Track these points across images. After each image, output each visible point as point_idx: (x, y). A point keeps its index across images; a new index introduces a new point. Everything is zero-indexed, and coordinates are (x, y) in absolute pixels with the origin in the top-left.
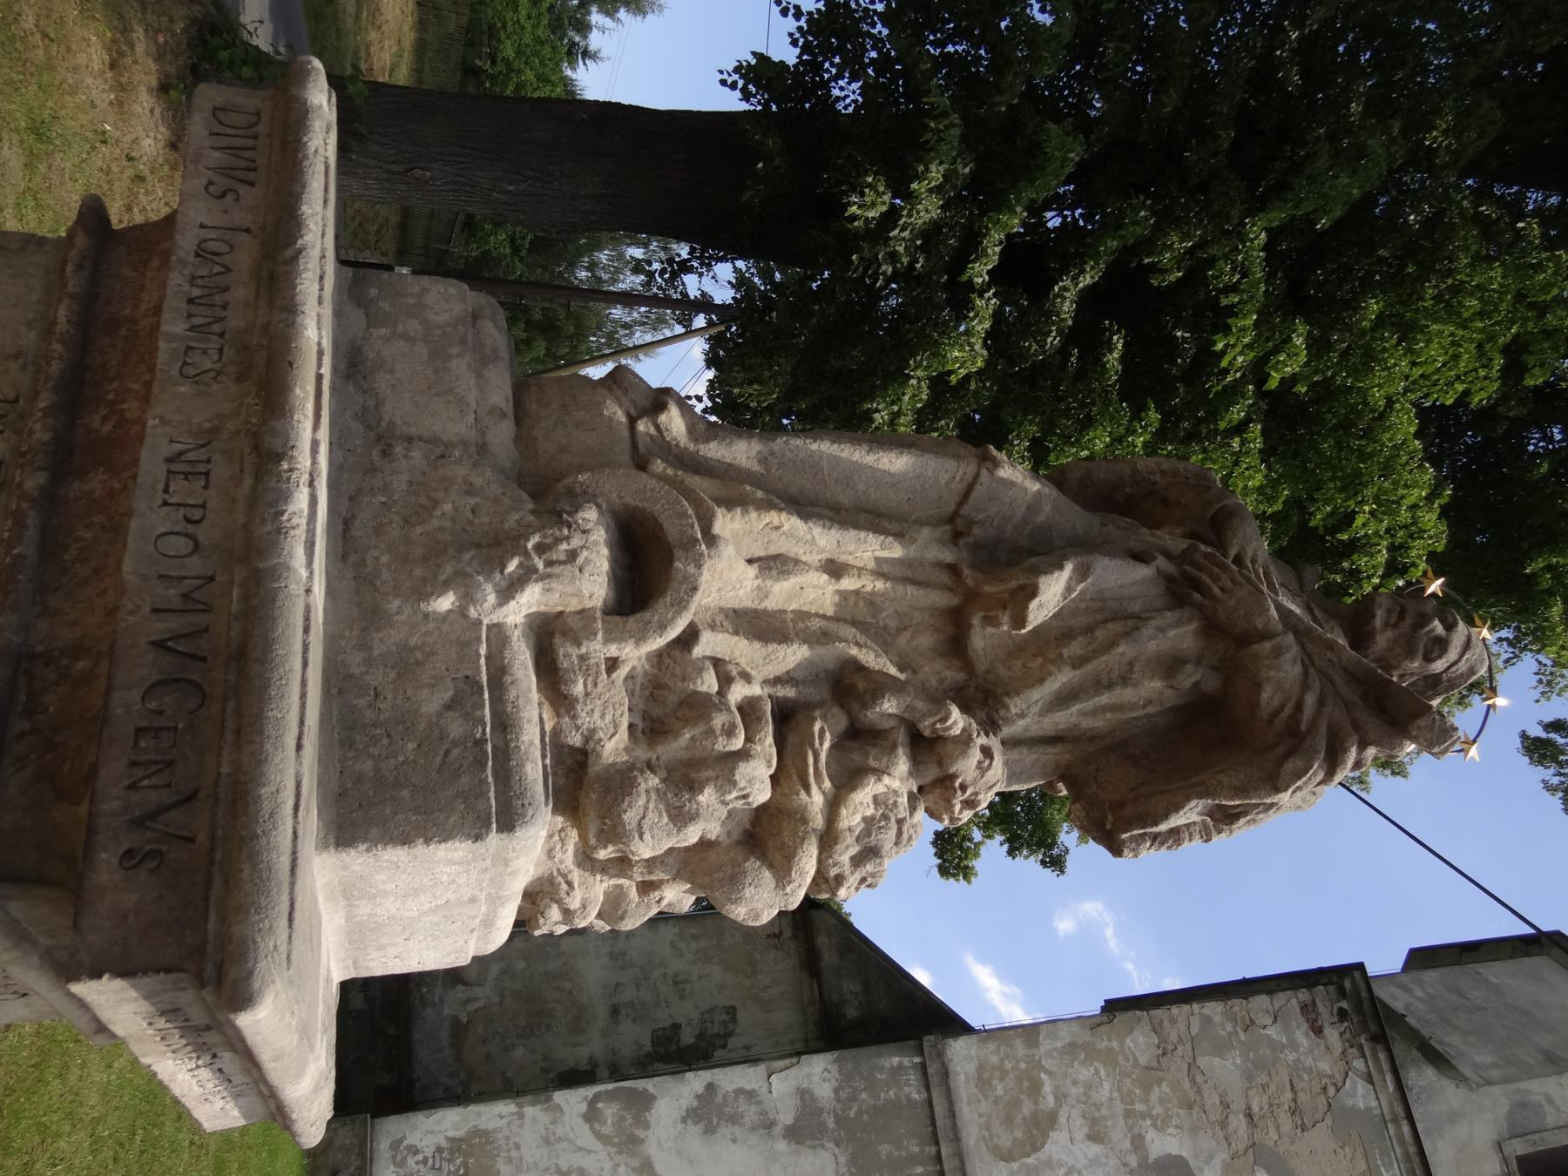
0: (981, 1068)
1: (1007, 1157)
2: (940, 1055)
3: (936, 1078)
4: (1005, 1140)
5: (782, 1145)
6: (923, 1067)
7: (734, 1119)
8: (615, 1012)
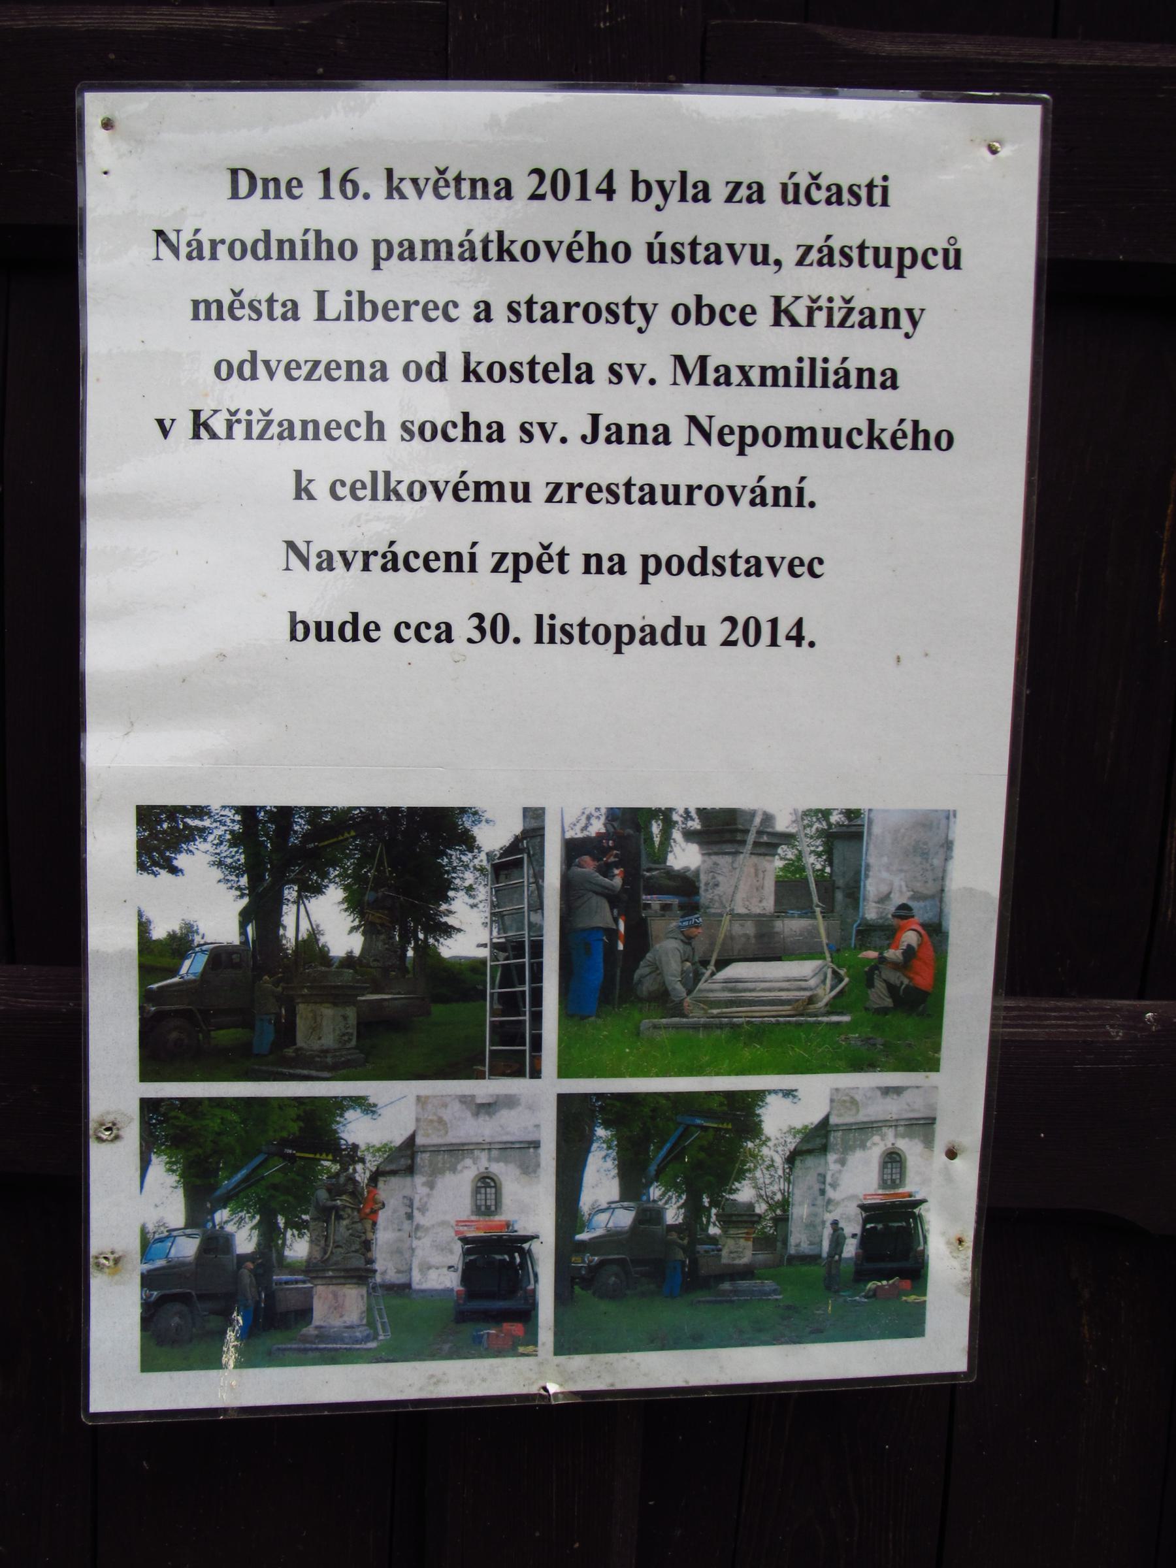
0: (423, 1136)
1: (447, 1132)
2: (420, 1146)
3: (425, 1149)
4: (442, 1132)
5: (434, 1192)
6: (421, 1152)
7: (426, 1203)
8: (399, 1230)
